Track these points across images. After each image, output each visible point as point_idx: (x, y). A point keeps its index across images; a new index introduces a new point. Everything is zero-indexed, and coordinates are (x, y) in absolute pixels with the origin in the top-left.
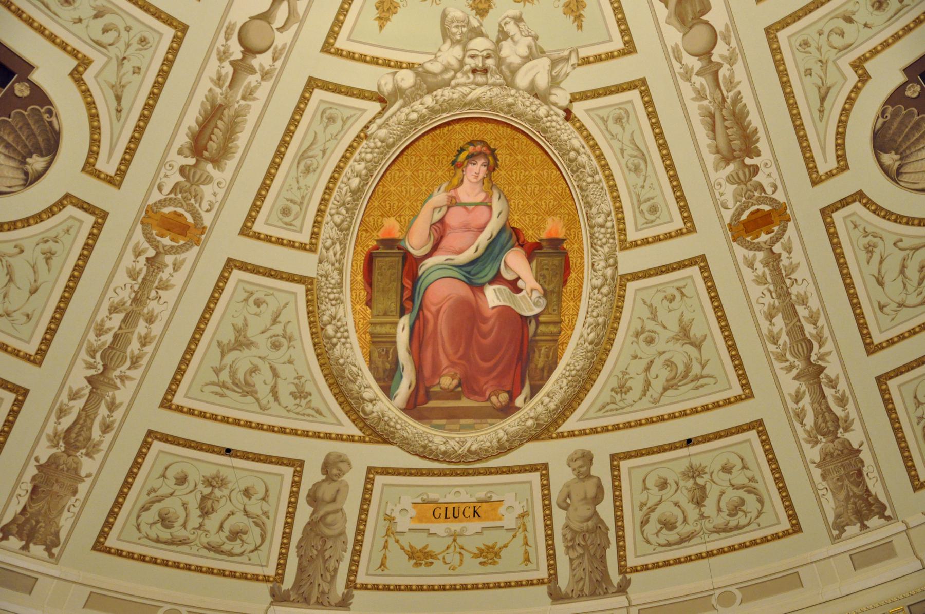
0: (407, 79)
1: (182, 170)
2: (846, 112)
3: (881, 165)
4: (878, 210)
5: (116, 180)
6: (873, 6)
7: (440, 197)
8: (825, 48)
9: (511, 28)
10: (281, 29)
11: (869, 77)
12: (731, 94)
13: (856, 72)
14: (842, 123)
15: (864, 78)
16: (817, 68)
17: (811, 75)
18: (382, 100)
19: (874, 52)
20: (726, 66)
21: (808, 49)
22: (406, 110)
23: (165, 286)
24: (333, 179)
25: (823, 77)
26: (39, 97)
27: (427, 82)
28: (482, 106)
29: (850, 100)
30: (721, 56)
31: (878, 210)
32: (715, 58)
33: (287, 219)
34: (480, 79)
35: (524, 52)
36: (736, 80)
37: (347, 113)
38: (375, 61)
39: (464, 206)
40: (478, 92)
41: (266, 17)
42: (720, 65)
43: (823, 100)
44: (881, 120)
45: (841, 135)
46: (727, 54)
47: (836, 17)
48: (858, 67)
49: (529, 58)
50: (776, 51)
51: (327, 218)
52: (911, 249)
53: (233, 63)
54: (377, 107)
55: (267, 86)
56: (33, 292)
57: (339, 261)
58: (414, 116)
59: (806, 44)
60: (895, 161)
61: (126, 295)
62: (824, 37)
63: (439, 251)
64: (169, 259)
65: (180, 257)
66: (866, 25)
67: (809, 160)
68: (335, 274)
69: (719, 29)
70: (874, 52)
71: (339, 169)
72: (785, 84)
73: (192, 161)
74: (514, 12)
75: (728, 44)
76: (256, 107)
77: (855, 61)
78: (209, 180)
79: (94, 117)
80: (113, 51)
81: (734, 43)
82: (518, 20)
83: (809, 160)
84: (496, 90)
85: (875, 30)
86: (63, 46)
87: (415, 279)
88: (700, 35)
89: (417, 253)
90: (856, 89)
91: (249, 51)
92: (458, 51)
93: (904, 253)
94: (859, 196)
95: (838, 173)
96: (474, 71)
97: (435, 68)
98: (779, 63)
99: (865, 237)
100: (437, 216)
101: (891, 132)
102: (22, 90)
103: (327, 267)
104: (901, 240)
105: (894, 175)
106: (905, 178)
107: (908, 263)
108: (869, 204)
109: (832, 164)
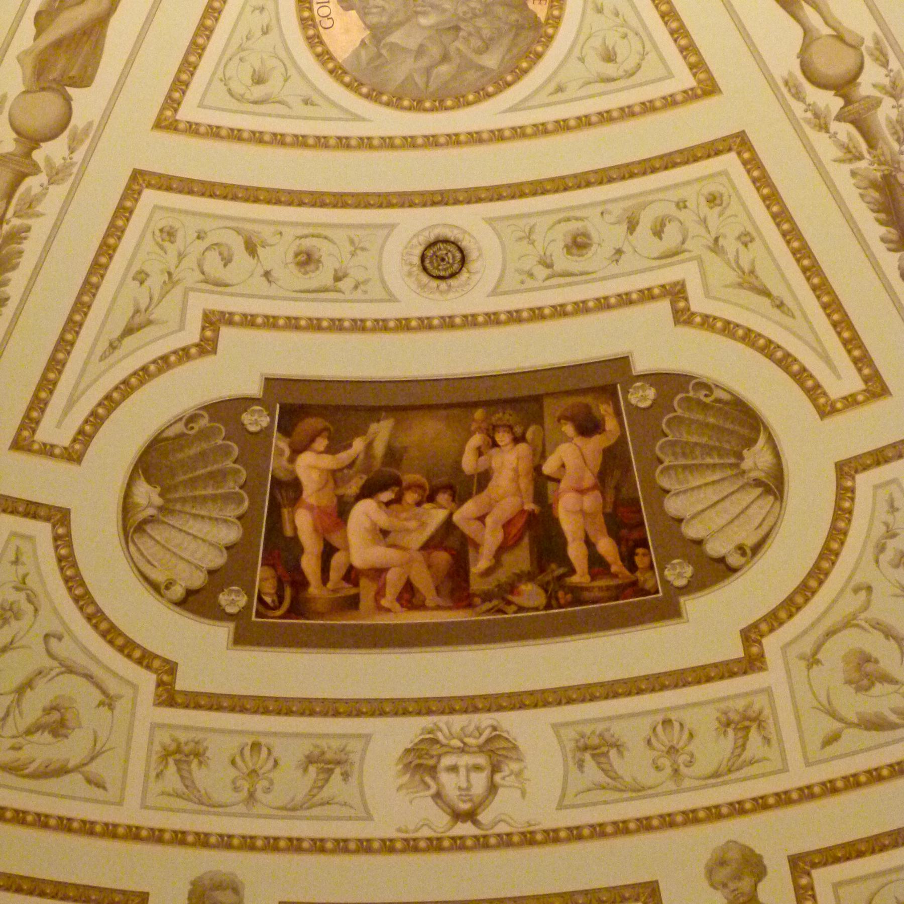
2: (144, 374)
3: (127, 495)
4: (66, 560)
6: (297, 255)
8: (190, 261)
11: (214, 351)
12: (17, 222)
13: (203, 328)
14: (126, 388)
15: (207, 346)
16: (156, 281)
17: (141, 283)
19: (249, 321)
20: (43, 178)
21: (167, 244)
25: (156, 298)
29: (164, 363)
30: (48, 159)
31: (66, 560)
32: (38, 156)
36: (40, 208)
42: (35, 170)
43: (129, 331)
44: (179, 428)
45: (110, 402)
46: (58, 162)
47: (238, 231)
48: (212, 323)
50: (123, 212)
52: (62, 664)
59: (170, 234)
60: (150, 505)
62: (202, 245)
66: (267, 274)
67: (38, 404)
69: (78, 120)
70: (249, 321)
72: (98, 268)
75: (72, 150)
77: (213, 312)
81: (78, 156)
83: (38, 404)
85: (273, 290)
88: (47, 106)
90: (184, 354)
93: (48, 662)
94: (59, 518)
95: (61, 457)
98: (115, 231)
99: (17, 589)
101: (180, 456)
104: (60, 638)
105: (133, 526)
106: (144, 543)
107: (41, 685)
108: (63, 540)
109: (63, 437)
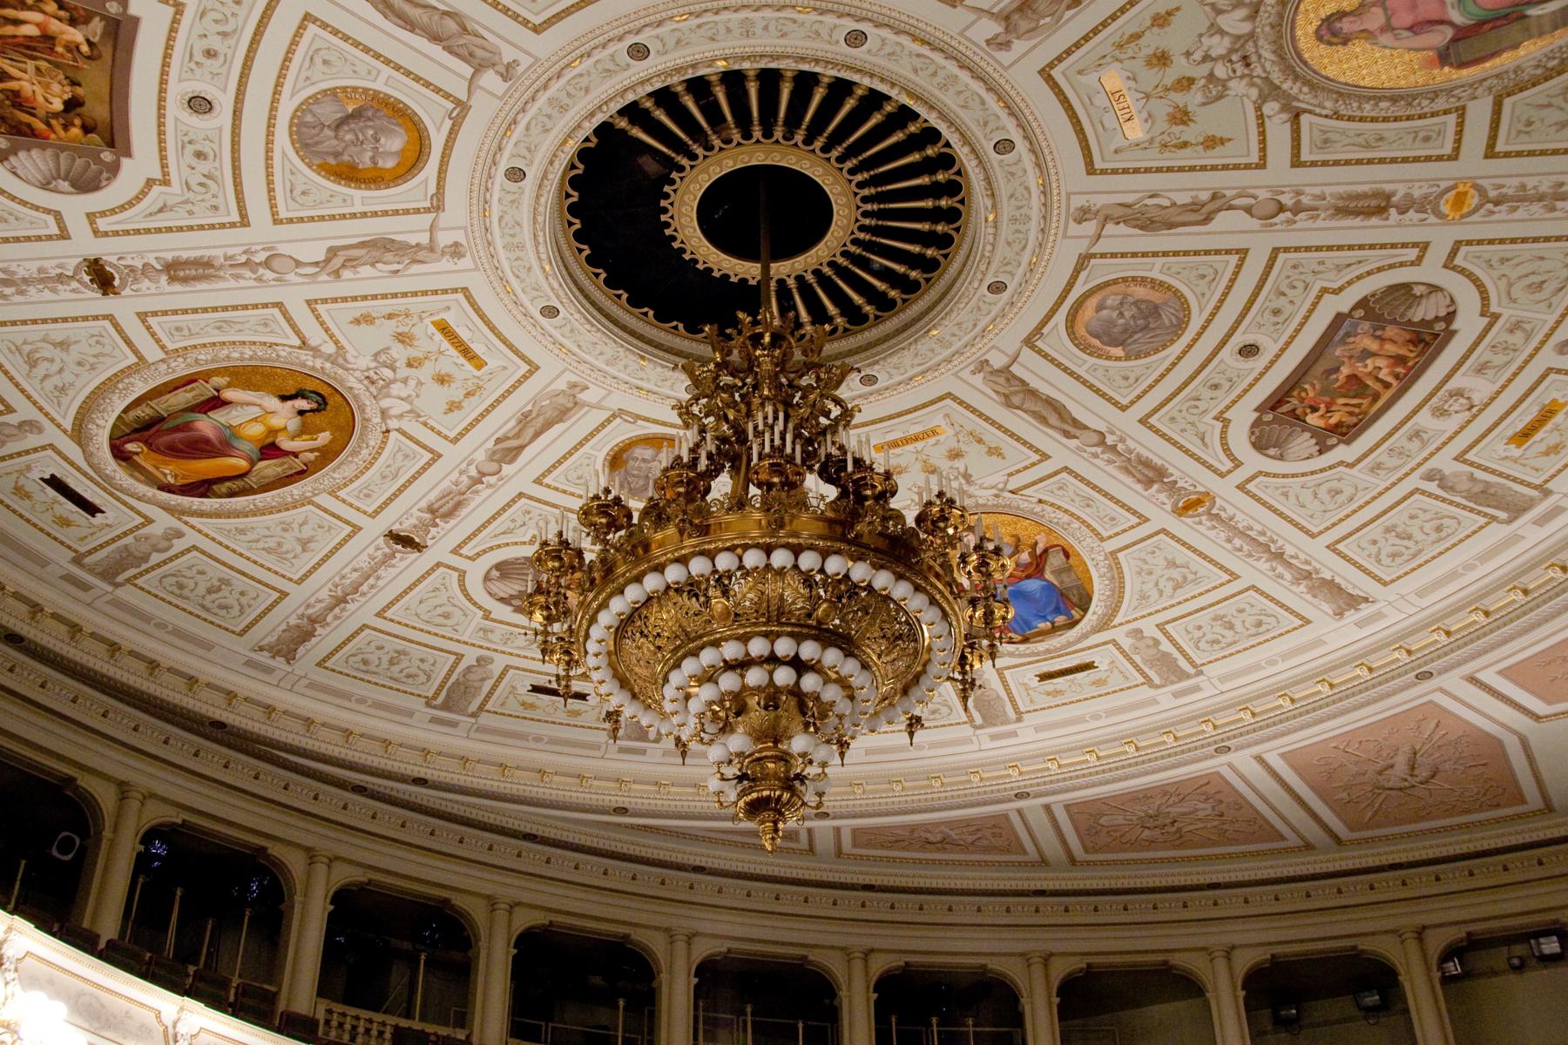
0: (1270, 108)
1: (1402, 212)
5: (1424, 247)
7: (1385, 39)
9: (1198, 56)
10: (1255, 197)
18: (1297, 116)
22: (1301, 97)
23: (1523, 187)
24: (1385, 120)
26: (1363, 303)
27: (1270, 90)
28: (1281, 47)
33: (1434, 135)
34: (1254, 58)
35: (1217, 38)
37: (1316, 132)
38: (1262, 134)
39: (1388, 19)
40: (1267, 54)
41: (1248, 210)
49: (1222, 32)
51: (1426, 110)
53: (1295, 215)
54: (1305, 119)
55: (1308, 190)
56: (1542, 258)
57: (1471, 86)
58: (1305, 89)
61: (1536, 208)
63: (1445, 18)
64: (1492, 194)
65: (1489, 188)
68: (1486, 84)
71: (1374, 120)
73: (1393, 211)
74: (1183, 60)
76: (1328, 190)
78: (1408, 196)
79: (1369, 273)
80: (1309, 278)
82: (1188, 54)
84: (1260, 43)
86: (1315, 305)
87: (1480, 24)
89: (1449, 33)
91: (1281, 208)
92: (1231, 84)
96: (1248, 65)
97: (1254, 93)
100: (1406, 34)
102: (1360, 313)
103: (1480, 91)
